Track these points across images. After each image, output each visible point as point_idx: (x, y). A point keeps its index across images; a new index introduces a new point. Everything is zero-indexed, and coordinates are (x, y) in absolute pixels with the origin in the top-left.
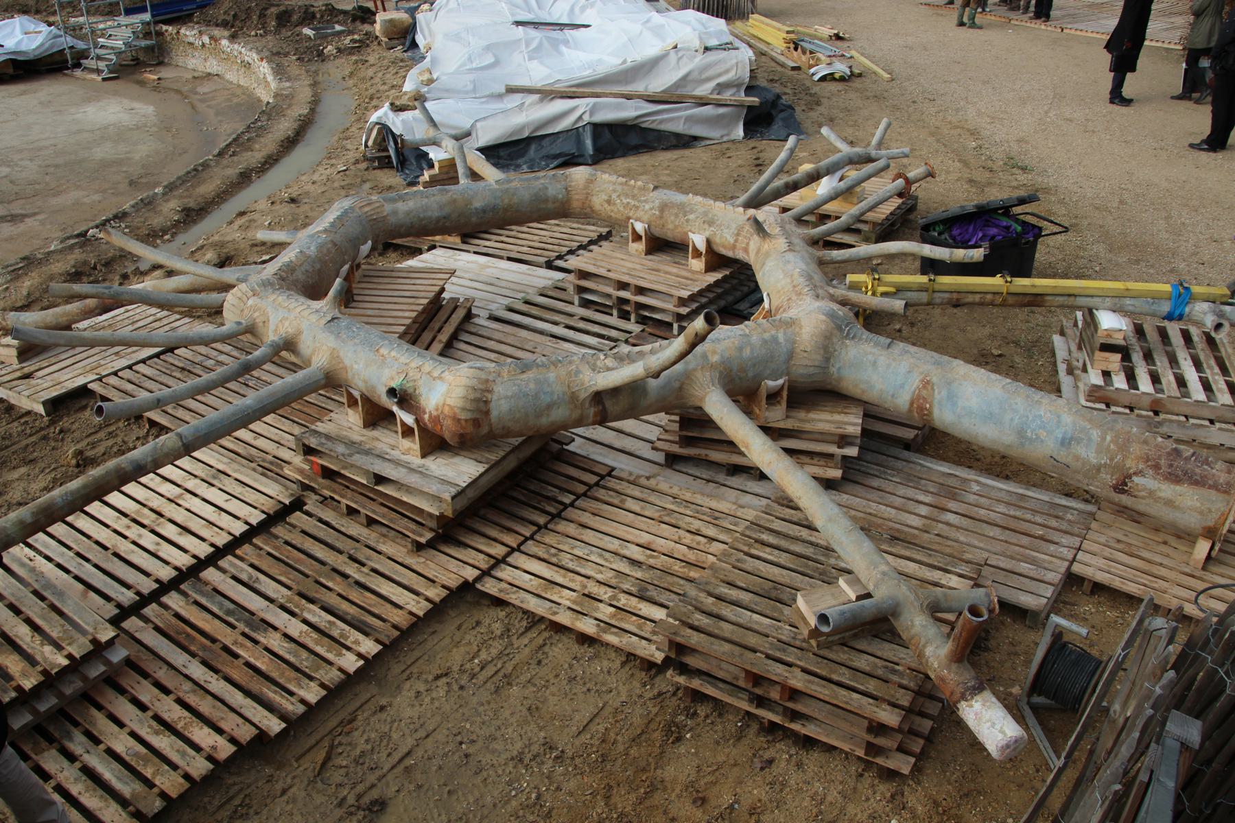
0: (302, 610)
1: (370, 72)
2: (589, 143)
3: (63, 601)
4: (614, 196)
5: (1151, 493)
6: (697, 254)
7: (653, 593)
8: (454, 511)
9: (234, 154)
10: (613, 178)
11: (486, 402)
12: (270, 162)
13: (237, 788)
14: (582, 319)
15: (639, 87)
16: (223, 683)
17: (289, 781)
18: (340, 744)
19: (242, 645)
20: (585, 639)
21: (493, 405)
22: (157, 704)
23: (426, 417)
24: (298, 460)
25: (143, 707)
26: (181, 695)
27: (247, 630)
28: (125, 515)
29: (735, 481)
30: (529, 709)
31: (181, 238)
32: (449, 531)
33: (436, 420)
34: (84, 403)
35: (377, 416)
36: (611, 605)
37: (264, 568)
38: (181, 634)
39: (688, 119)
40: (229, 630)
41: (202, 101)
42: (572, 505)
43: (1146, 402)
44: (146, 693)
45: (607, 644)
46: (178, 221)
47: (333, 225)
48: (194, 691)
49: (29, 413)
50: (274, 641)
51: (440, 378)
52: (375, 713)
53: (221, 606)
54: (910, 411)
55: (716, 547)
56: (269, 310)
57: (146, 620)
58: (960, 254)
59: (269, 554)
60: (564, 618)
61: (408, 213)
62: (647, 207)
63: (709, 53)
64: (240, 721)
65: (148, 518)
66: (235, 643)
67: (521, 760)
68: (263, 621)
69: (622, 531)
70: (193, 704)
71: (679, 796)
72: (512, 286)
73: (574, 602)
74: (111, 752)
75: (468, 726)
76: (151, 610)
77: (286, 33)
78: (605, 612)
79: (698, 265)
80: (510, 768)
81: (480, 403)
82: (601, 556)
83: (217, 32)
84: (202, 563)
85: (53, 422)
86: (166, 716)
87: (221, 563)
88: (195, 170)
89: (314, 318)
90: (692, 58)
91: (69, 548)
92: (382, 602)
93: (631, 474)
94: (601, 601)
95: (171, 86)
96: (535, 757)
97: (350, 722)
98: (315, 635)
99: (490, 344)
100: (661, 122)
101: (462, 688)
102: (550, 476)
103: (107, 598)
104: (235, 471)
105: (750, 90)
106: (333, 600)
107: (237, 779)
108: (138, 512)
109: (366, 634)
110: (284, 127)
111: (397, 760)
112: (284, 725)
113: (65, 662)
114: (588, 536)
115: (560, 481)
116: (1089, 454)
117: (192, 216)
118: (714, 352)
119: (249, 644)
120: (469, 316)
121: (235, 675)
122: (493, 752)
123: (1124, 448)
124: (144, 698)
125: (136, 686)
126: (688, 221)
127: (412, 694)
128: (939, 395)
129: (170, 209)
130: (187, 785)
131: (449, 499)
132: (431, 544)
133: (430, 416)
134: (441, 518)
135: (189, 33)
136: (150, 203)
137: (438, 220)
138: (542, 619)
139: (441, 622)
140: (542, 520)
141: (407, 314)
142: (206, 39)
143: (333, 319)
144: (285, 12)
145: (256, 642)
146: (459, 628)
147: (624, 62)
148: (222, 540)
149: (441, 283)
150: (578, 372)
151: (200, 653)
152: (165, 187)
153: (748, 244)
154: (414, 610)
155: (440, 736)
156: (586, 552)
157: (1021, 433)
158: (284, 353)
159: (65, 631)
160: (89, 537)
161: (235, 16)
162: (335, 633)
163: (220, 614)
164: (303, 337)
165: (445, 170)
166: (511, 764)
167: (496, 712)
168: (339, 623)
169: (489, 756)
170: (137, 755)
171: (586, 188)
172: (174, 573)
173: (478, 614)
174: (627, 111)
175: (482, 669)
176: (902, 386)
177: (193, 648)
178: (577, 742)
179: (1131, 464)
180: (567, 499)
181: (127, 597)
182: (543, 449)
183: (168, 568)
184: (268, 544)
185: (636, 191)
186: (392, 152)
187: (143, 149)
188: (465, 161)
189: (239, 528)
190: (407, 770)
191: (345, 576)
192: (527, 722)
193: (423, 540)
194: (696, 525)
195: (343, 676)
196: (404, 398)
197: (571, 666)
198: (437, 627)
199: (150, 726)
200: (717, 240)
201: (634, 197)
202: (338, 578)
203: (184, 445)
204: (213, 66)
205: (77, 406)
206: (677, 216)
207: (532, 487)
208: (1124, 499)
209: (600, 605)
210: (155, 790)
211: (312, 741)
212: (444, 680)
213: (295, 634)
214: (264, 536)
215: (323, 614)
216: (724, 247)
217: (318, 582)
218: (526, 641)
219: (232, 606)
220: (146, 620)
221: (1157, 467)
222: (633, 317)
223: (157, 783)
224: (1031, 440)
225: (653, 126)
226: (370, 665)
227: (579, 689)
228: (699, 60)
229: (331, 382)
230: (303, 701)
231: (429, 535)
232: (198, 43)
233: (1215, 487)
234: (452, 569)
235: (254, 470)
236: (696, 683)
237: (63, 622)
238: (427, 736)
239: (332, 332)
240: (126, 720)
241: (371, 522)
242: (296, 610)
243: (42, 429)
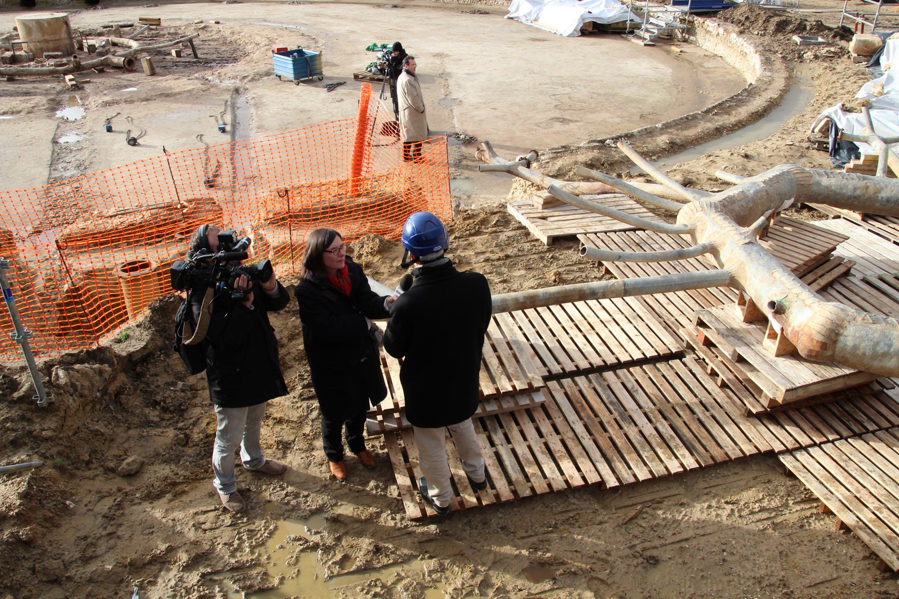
0: (657, 421)
1: (834, 78)
3: (521, 355)
8: (784, 400)
9: (716, 114)
11: (838, 335)
12: (740, 125)
13: (575, 507)
16: (592, 442)
17: (606, 518)
18: (646, 513)
19: (612, 426)
21: (842, 338)
22: (550, 436)
23: (790, 329)
24: (691, 327)
25: (541, 435)
26: (565, 438)
27: (618, 418)
28: (573, 321)
30: (781, 553)
31: (662, 162)
32: (775, 414)
33: (796, 334)
34: (571, 245)
35: (756, 317)
36: (874, 513)
38: (579, 403)
40: (608, 413)
41: (705, 72)
42: (873, 432)
44: (546, 427)
45: (859, 538)
46: (665, 149)
47: (771, 180)
48: (573, 439)
49: (537, 240)
50: (633, 432)
51: (810, 306)
52: (677, 504)
57: (562, 386)
59: (650, 378)
60: (833, 506)
61: (827, 187)
64: (593, 469)
65: (585, 327)
66: (608, 422)
67: (760, 582)
68: (630, 417)
70: (570, 446)
73: (845, 498)
74: (514, 451)
75: (733, 542)
76: (566, 382)
77: (780, 36)
80: (750, 583)
81: (833, 334)
82: (881, 476)
83: (730, 27)
84: (606, 367)
85: (549, 250)
86: (551, 446)
87: (618, 371)
88: (687, 118)
89: (737, 237)
91: (534, 327)
92: (710, 438)
94: (867, 507)
95: (688, 58)
96: (771, 585)
97: (659, 502)
98: (659, 440)
101: (740, 516)
102: (864, 406)
103: (545, 364)
104: (648, 319)
106: (679, 424)
107: (576, 502)
108: (580, 321)
109: (692, 454)
110: (757, 104)
111: (677, 539)
112: (617, 484)
113: (511, 389)
115: (871, 413)
117: (674, 148)
119: (617, 427)
120: (847, 273)
121: (601, 442)
122: (743, 567)
124: (544, 430)
125: (542, 421)
127: (706, 505)
129: (662, 140)
130: (548, 490)
131: (784, 391)
132: (760, 417)
133: (793, 330)
134: (773, 402)
135: (711, 24)
136: (650, 132)
137: (850, 197)
138: (817, 500)
139: (744, 469)
140: (845, 433)
141: (801, 257)
142: (721, 30)
143: (749, 243)
144: (784, 21)
145: (621, 428)
146: (755, 478)
148: (624, 358)
149: (835, 243)
151: (585, 419)
152: (664, 125)
154: (729, 453)
155: (712, 539)
156: (871, 469)
158: (708, 255)
159: (517, 372)
160: (547, 325)
161: (747, 18)
162: (672, 444)
163: (606, 402)
165: (868, 163)
166: (752, 581)
167: (756, 543)
168: (677, 439)
169: (739, 568)
170: (527, 459)
172: (588, 366)
173: (771, 476)
175: (759, 511)
177: (582, 414)
178: (806, 591)
180: (871, 427)
181: (556, 369)
182: (866, 385)
183: (586, 361)
184: (651, 372)
186: (831, 140)
187: (657, 97)
188: (886, 160)
189: (637, 355)
191: (693, 412)
192: (775, 561)
193: (754, 411)
195: (666, 473)
196: (779, 309)
197: (824, 540)
198: (738, 469)
199: (541, 447)
202: (688, 412)
203: (625, 289)
204: (720, 50)
205: (566, 246)
207: (847, 409)
209: (865, 509)
210: (529, 484)
211: (630, 502)
212: (731, 506)
213: (647, 434)
214: (651, 366)
215: (669, 429)
217: (673, 408)
218: (798, 508)
219: (615, 400)
220: (562, 386)
223: (532, 480)
226: (686, 474)
227: (823, 557)
229: (732, 282)
230: (635, 476)
231: (760, 409)
232: (715, 32)
234: (767, 437)
235: (660, 323)
237: (517, 366)
238: (704, 535)
239: (746, 251)
240: (529, 437)
242: (654, 420)
243: (542, 252)
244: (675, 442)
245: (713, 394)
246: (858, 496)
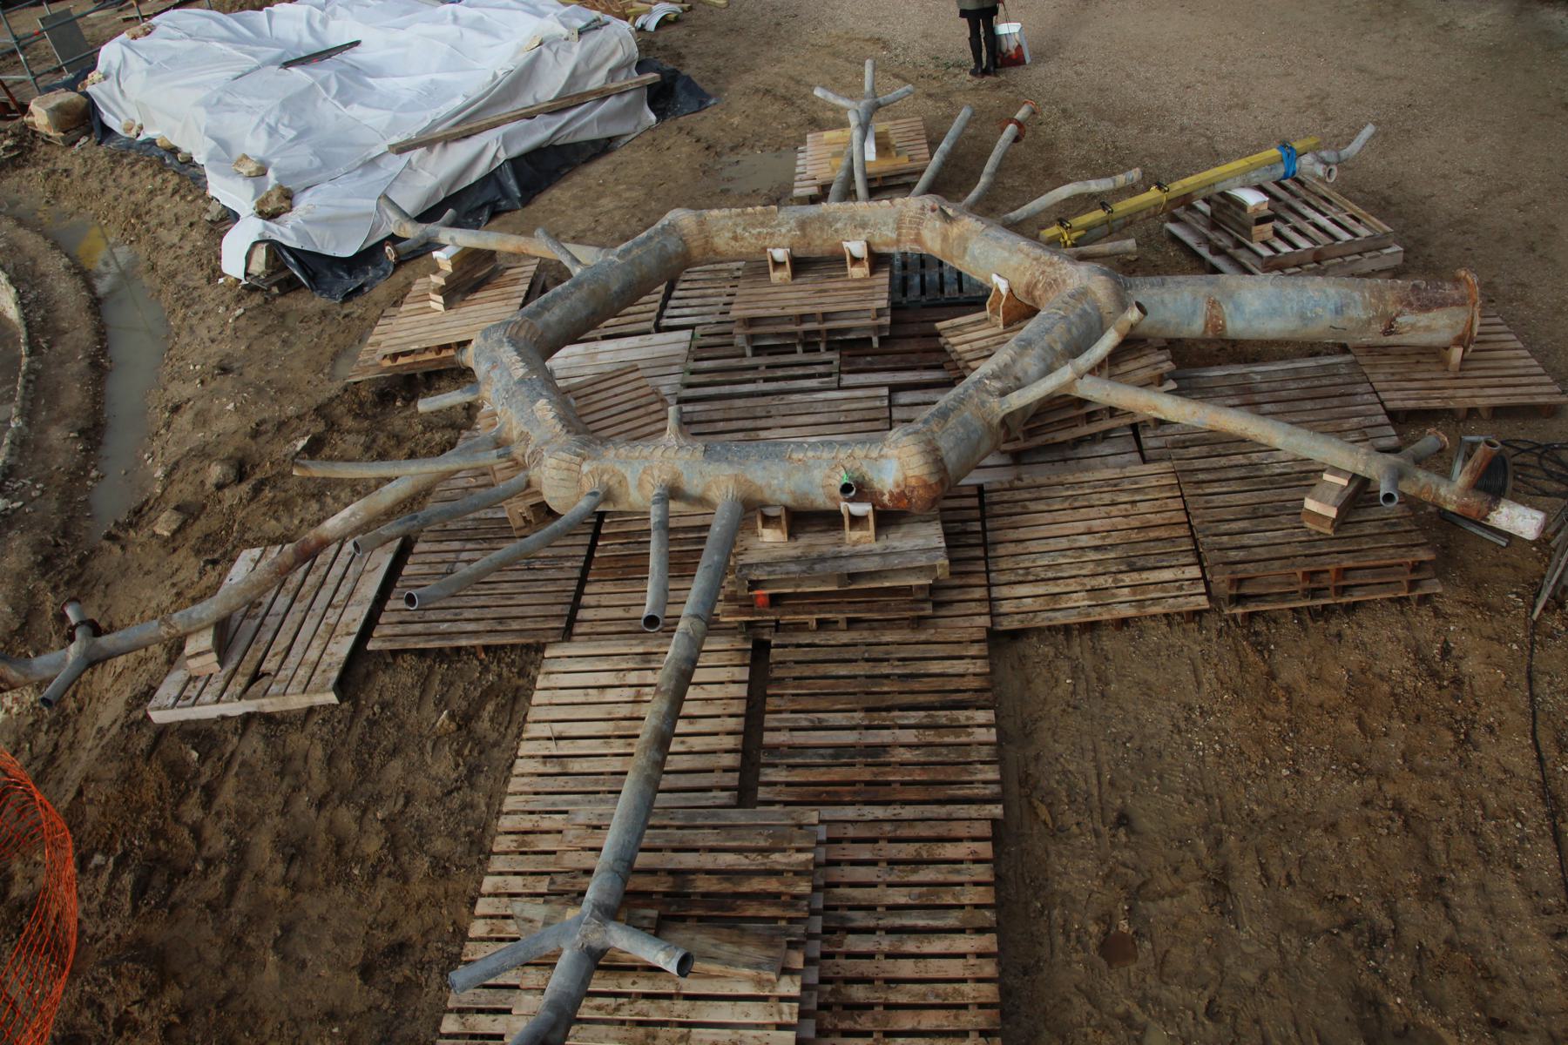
4: (739, 230)
5: (1413, 326)
6: (856, 261)
7: (1140, 563)
10: (726, 212)
11: (942, 460)
14: (768, 367)
15: (526, 101)
19: (884, 773)
20: (1123, 623)
23: (886, 498)
29: (1083, 451)
37: (810, 707)
39: (602, 119)
43: (1310, 257)
53: (822, 756)
54: (1205, 332)
55: (1143, 507)
56: (618, 467)
58: (1121, 179)
61: (560, 322)
62: (784, 230)
63: (586, 37)
69: (1055, 530)
71: (1309, 689)
79: (858, 272)
90: (569, 50)
99: (721, 426)
100: (576, 132)
105: (642, 67)
114: (1033, 546)
116: (1358, 313)
123: (1381, 298)
126: (836, 231)
128: (1227, 308)
133: (891, 494)
145: (888, 764)
147: (495, 76)
150: (983, 403)
153: (918, 234)
157: (1302, 317)
163: (830, 761)
164: (685, 478)
170: (920, 896)
174: (540, 132)
176: (1194, 313)
179: (1392, 309)
190: (1112, 783)
194: (1107, 498)
196: (856, 489)
200: (877, 239)
201: (762, 224)
206: (821, 229)
208: (1392, 339)
216: (887, 245)
219: (830, 751)
221: (1410, 304)
222: (822, 348)
224: (1311, 319)
225: (570, 140)
228: (578, 49)
233: (1454, 304)
236: (1252, 608)
241: (852, 623)
244: (942, 716)
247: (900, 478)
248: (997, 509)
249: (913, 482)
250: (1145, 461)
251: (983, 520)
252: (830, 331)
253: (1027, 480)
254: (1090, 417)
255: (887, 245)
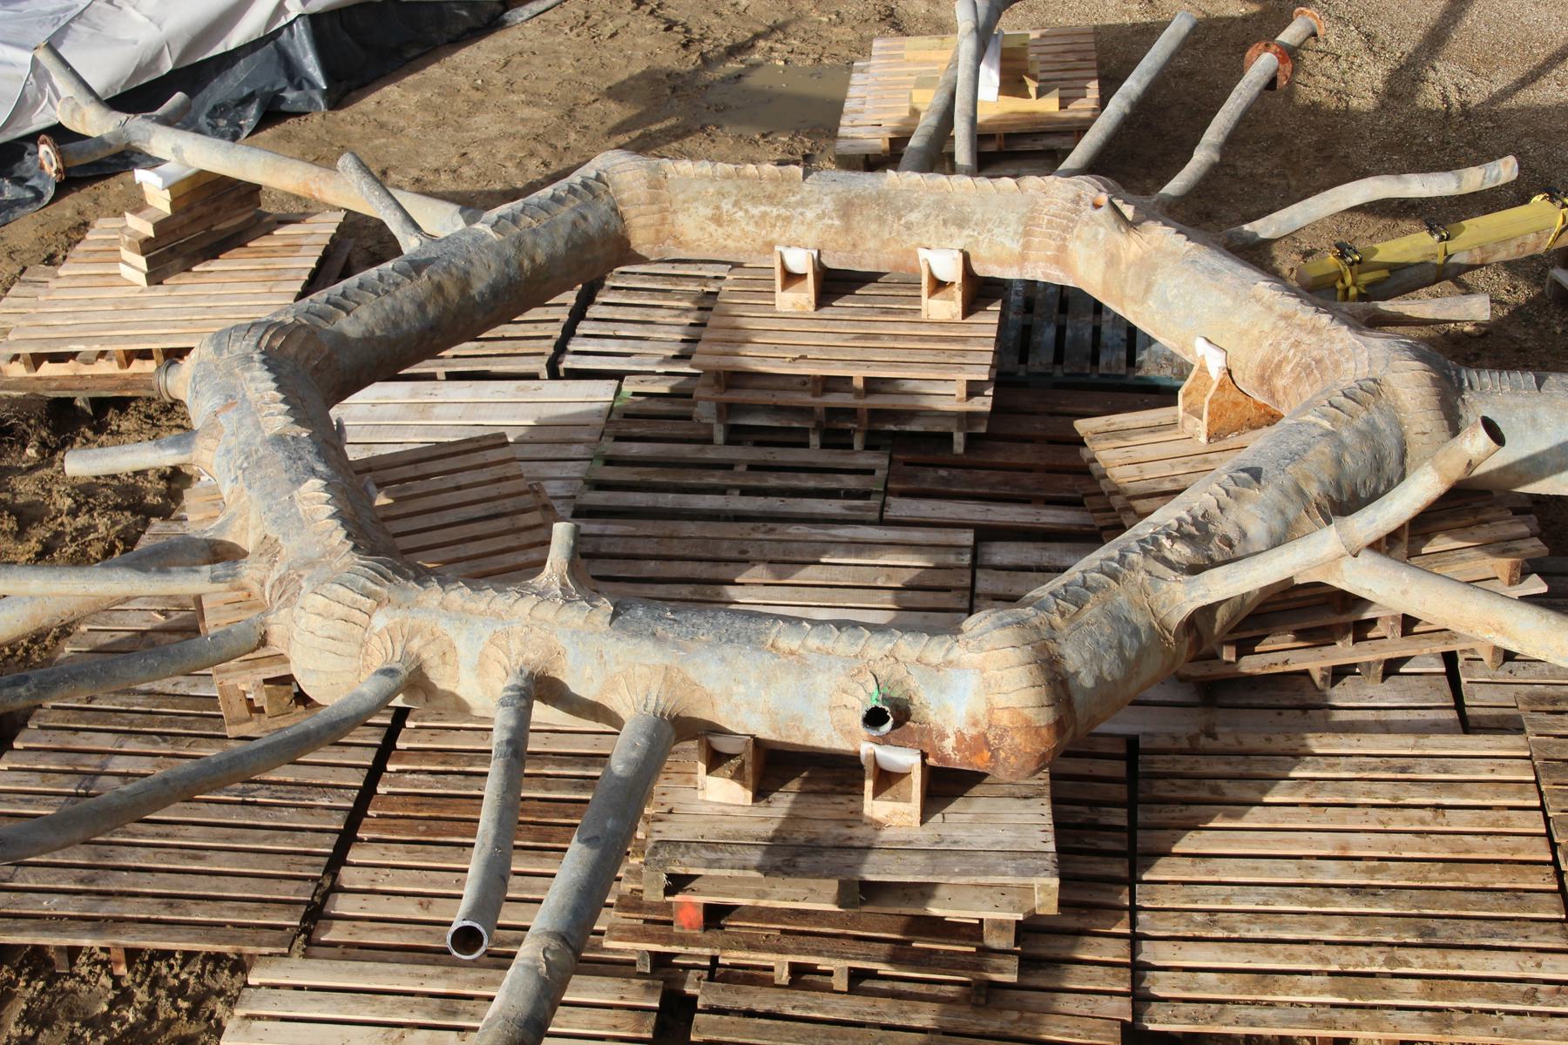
2: (311, 65)
4: (726, 205)
6: (938, 285)
7: (1445, 933)
10: (705, 167)
14: (753, 467)
23: (949, 744)
29: (1340, 695)
55: (1458, 821)
58: (1474, 179)
61: (368, 339)
72: (557, 434)
78: (1410, 994)
79: (946, 308)
93: (1175, 738)
99: (650, 568)
118: (1307, 478)
126: (909, 226)
133: (960, 738)
153: (1062, 249)
171: (654, 200)
185: (770, 188)
194: (1383, 796)
201: (771, 199)
206: (881, 220)
222: (858, 442)
245: (869, 1019)
246: (1335, 968)
247: (981, 709)
248: (1162, 788)
249: (1004, 719)
250: (1467, 725)
251: (1131, 805)
252: (876, 414)
253: (1226, 739)
254: (1361, 630)
255: (1001, 263)
